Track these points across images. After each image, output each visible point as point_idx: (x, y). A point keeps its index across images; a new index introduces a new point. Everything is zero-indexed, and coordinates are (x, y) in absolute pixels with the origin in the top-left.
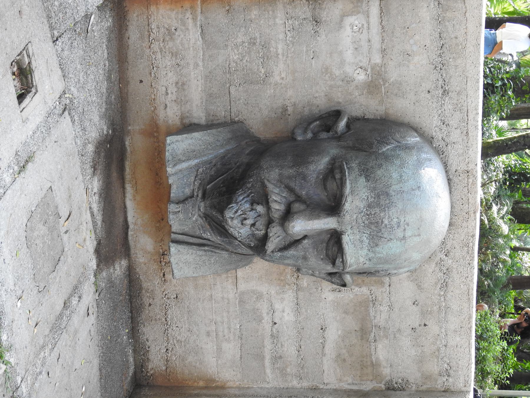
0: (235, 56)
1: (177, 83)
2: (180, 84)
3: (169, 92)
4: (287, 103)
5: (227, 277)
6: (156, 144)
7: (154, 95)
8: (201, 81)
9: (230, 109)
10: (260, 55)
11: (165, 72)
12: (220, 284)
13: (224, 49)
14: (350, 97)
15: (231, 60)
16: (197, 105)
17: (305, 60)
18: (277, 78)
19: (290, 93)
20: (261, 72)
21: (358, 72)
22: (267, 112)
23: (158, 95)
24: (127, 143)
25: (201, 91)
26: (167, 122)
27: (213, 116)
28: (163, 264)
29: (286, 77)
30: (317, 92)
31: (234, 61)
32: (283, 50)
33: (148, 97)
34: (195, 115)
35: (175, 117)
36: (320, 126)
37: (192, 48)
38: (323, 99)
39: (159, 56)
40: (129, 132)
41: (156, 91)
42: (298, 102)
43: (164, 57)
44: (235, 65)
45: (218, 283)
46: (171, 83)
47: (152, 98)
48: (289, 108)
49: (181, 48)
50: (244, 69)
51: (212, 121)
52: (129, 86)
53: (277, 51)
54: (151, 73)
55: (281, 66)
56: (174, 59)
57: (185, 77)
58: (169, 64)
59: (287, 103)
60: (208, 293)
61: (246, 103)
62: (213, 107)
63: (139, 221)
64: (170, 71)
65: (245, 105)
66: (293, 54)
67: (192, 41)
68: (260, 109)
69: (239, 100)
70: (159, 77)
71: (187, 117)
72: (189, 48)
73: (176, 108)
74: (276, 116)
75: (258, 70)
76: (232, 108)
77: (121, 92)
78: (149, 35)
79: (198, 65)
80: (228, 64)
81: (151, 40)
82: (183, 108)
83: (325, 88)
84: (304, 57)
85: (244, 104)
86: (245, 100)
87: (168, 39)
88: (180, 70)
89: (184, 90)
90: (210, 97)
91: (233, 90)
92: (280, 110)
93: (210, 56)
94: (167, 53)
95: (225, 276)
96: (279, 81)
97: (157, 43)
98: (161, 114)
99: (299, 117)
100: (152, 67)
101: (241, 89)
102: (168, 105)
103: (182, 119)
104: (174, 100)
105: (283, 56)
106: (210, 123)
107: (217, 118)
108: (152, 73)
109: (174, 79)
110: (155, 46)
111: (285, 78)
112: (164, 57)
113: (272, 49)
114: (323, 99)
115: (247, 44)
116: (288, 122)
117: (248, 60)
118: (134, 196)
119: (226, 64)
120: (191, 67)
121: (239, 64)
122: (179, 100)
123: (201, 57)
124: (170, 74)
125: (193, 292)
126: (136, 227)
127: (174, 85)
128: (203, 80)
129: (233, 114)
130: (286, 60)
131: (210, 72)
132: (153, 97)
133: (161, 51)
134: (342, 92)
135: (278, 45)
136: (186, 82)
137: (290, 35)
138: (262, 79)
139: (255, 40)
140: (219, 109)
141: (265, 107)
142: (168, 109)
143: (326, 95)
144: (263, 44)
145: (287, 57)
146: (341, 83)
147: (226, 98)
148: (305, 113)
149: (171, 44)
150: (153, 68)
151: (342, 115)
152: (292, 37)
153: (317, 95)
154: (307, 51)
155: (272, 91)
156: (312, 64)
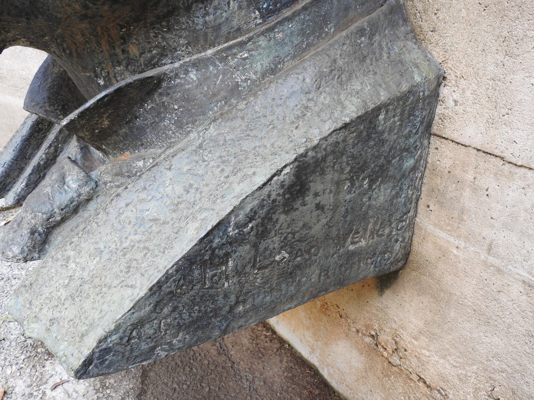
5: (475, 189)
12: (492, 226)
28: (395, 360)
45: (485, 232)
60: (516, 288)
63: (308, 335)
95: (467, 193)
125: (495, 339)
126: (317, 354)
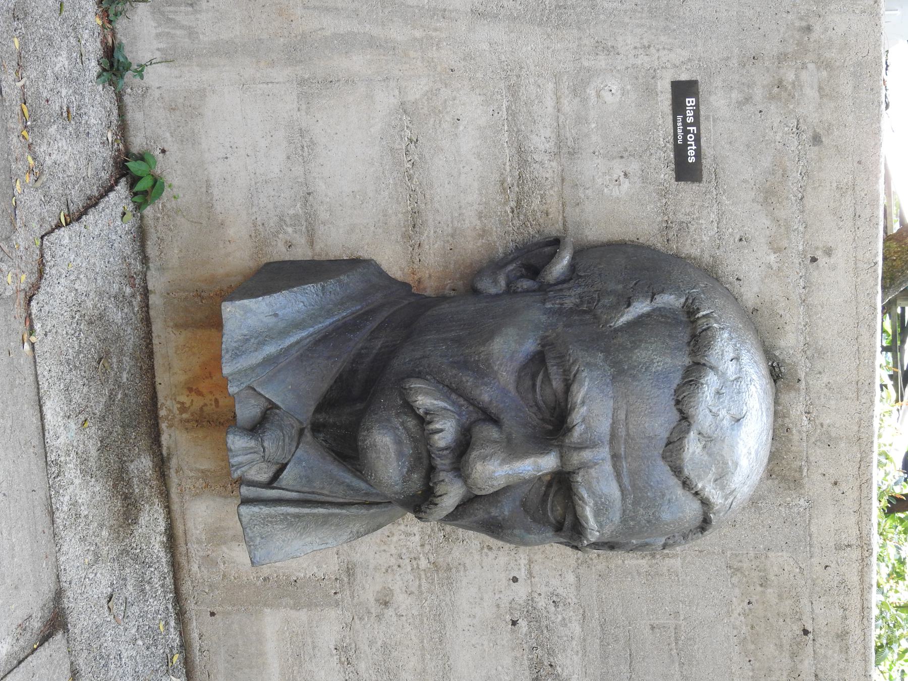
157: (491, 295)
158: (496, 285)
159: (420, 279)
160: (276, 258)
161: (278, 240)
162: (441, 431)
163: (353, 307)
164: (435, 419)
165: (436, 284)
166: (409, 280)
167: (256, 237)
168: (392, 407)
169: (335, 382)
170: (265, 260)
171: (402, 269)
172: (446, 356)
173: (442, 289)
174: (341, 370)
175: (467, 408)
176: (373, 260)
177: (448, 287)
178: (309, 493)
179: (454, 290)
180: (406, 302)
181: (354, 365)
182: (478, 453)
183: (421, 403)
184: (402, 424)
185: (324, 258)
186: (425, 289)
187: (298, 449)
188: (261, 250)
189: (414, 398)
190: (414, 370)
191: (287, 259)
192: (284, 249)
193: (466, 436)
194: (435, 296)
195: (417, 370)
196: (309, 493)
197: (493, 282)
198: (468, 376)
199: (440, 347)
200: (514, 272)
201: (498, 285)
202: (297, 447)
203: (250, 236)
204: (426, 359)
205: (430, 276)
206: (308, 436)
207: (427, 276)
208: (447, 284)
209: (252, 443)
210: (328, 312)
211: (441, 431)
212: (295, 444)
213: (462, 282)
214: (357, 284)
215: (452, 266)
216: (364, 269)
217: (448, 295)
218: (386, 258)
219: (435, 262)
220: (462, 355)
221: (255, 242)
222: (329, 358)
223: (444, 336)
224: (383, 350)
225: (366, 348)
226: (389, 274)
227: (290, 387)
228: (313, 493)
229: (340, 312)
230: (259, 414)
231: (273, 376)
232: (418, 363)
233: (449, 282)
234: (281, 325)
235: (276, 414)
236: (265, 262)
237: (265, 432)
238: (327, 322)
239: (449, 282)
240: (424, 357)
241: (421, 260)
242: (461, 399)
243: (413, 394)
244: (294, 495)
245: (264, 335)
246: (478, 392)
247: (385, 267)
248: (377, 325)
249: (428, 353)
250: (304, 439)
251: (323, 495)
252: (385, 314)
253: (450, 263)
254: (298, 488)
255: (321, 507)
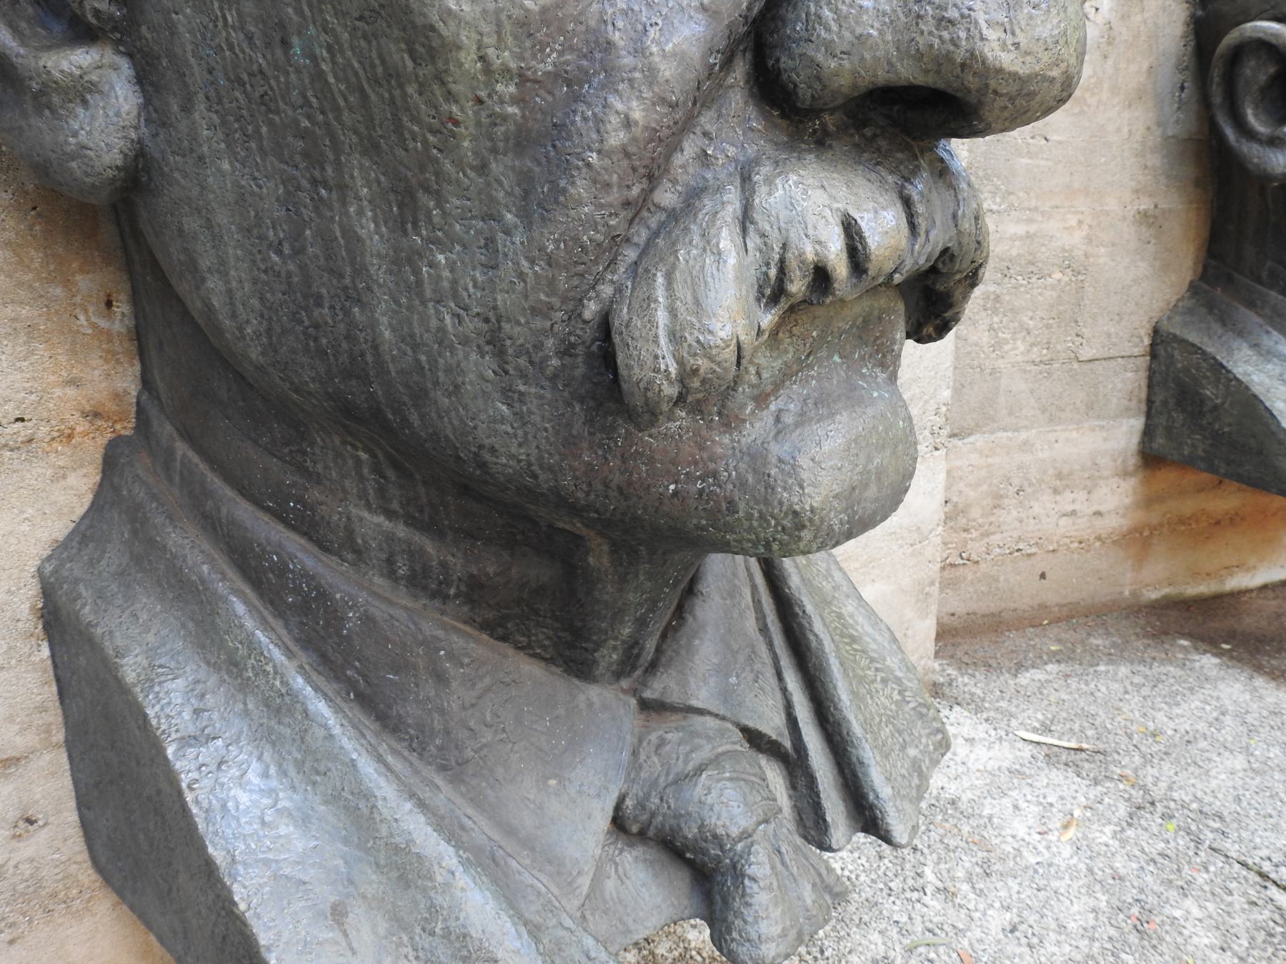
0: (1017, 348)
1: (1056, 491)
2: (1058, 483)
3: (1069, 508)
4: (1131, 210)
6: (1165, 530)
7: (1072, 542)
8: (1058, 434)
9: (1122, 357)
10: (1025, 282)
11: (1032, 521)
13: (1000, 378)
14: (1143, 38)
15: (1025, 358)
16: (1105, 440)
17: (1047, 159)
18: (1078, 237)
19: (1112, 204)
20: (1059, 281)
21: (1094, 10)
22: (1141, 264)
23: (1074, 534)
24: (1154, 595)
25: (1078, 430)
26: (1127, 508)
27: (1130, 400)
29: (1077, 212)
30: (1119, 130)
31: (1029, 351)
32: (1019, 221)
33: (1076, 556)
34: (1123, 443)
35: (1119, 490)
36: (1256, 107)
37: (990, 460)
38: (1137, 114)
39: (996, 539)
40: (1133, 594)
41: (1065, 540)
42: (1133, 183)
43: (999, 526)
44: (1035, 349)
46: (1054, 505)
47: (1078, 548)
48: (1142, 207)
49: (985, 487)
50: (1048, 327)
51: (1140, 402)
52: (1048, 604)
53: (1021, 238)
54: (1029, 555)
55: (1053, 226)
56: (1006, 501)
57: (1045, 472)
58: (1014, 513)
59: (1132, 213)
61: (1117, 318)
62: (1114, 400)
64: (1030, 511)
65: (1121, 319)
66: (1032, 194)
67: (975, 459)
68: (1136, 281)
69: (1109, 335)
70: (1039, 534)
71: (1124, 461)
72: (989, 466)
73: (1105, 490)
74: (1153, 241)
75: (1053, 288)
76: (1123, 354)
77: (1058, 620)
78: (953, 565)
79: (1025, 443)
80: (1033, 367)
81: (961, 562)
82: (1106, 473)
83: (1114, 106)
84: (1042, 163)
85: (1118, 322)
86: (1111, 320)
87: (964, 521)
88: (1031, 485)
89: (1070, 474)
90: (1091, 408)
91: (1086, 353)
92: (1144, 229)
93: (1011, 413)
94: (992, 519)
96: (1084, 233)
97: (969, 547)
98: (1114, 523)
99: (1163, 180)
100: (1016, 554)
101: (1086, 332)
102: (1095, 508)
103: (1125, 474)
104: (1086, 496)
105: (1031, 221)
106: (1144, 407)
107: (1137, 390)
108: (1029, 552)
109: (1046, 497)
110: (975, 549)
111: (1080, 216)
112: (999, 526)
113: (1014, 252)
114: (1137, 114)
115: (996, 319)
116: (1170, 210)
117: (1030, 314)
118: (1248, 570)
119: (1030, 371)
120: (1027, 458)
121: (1036, 336)
122: (1089, 483)
123: (1010, 434)
124: (1037, 509)
127: (1058, 498)
128: (1059, 428)
129: (1136, 351)
130: (1043, 213)
131: (1043, 412)
132: (1076, 545)
133: (988, 535)
134: (1128, 60)
135: (1008, 235)
136: (1055, 468)
137: (989, 202)
138: (1074, 279)
139: (988, 297)
140: (1120, 386)
141: (1132, 268)
142: (1103, 508)
143: (1130, 106)
144: (999, 275)
145: (1036, 209)
146: (1110, 62)
147: (1101, 368)
148: (1158, 163)
149: (975, 513)
150: (1019, 550)
151: (1261, 35)
152: (994, 194)
153: (1125, 130)
154: (1030, 155)
155: (1103, 250)
156: (1060, 143)
157: (147, 104)
158: (93, 88)
159: (85, 415)
160: (75, 845)
161: (12, 863)
162: (851, 230)
163: (241, 626)
164: (810, 256)
165: (96, 362)
166: (94, 448)
167: (12, 925)
168: (702, 448)
169: (504, 639)
170: (87, 875)
171: (60, 475)
172: (490, 241)
173: (110, 341)
174: (468, 629)
175: (706, 134)
176: (40, 571)
177: (103, 323)
178: (770, 645)
179: (109, 304)
180: (181, 448)
181: (452, 591)
182: (992, 35)
183: (742, 322)
184: (761, 400)
185: (54, 716)
186: (117, 396)
187: (695, 703)
188: (53, 895)
189: (729, 355)
190: (554, 378)
191: (73, 817)
192: (43, 836)
193: (826, 133)
194: (137, 363)
195: (555, 362)
196: (770, 645)
197: (85, 102)
198: (599, 121)
199: (439, 278)
200: (23, 25)
201: (94, 78)
202: (701, 712)
203: (11, 942)
204: (506, 326)
205: (73, 382)
206: (661, 686)
207: (71, 392)
208: (94, 326)
209: (759, 865)
210: (278, 710)
211: (851, 230)
212: (697, 720)
213: (78, 277)
214: (144, 616)
215: (25, 312)
216: (79, 596)
217: (130, 322)
218: (25, 527)
219: (20, 370)
220: (482, 169)
221: (30, 921)
222: (440, 678)
223: (379, 271)
224: (395, 505)
225: (390, 561)
226: (80, 510)
227: (553, 782)
228: (764, 630)
229: (269, 668)
230: (639, 851)
231: (533, 849)
232: (522, 361)
233: (82, 318)
234: (372, 882)
235: (641, 805)
236: (91, 871)
237: (715, 836)
238: (320, 707)
239: (82, 318)
240: (495, 342)
241: (17, 414)
242: (678, 159)
243: (711, 359)
244: (793, 682)
245: (426, 941)
246: (667, 70)
247: (60, 528)
248: (294, 536)
249: (471, 325)
250: (675, 697)
251: (757, 603)
252: (243, 512)
253: (14, 320)
254: (769, 672)
255: (802, 607)
